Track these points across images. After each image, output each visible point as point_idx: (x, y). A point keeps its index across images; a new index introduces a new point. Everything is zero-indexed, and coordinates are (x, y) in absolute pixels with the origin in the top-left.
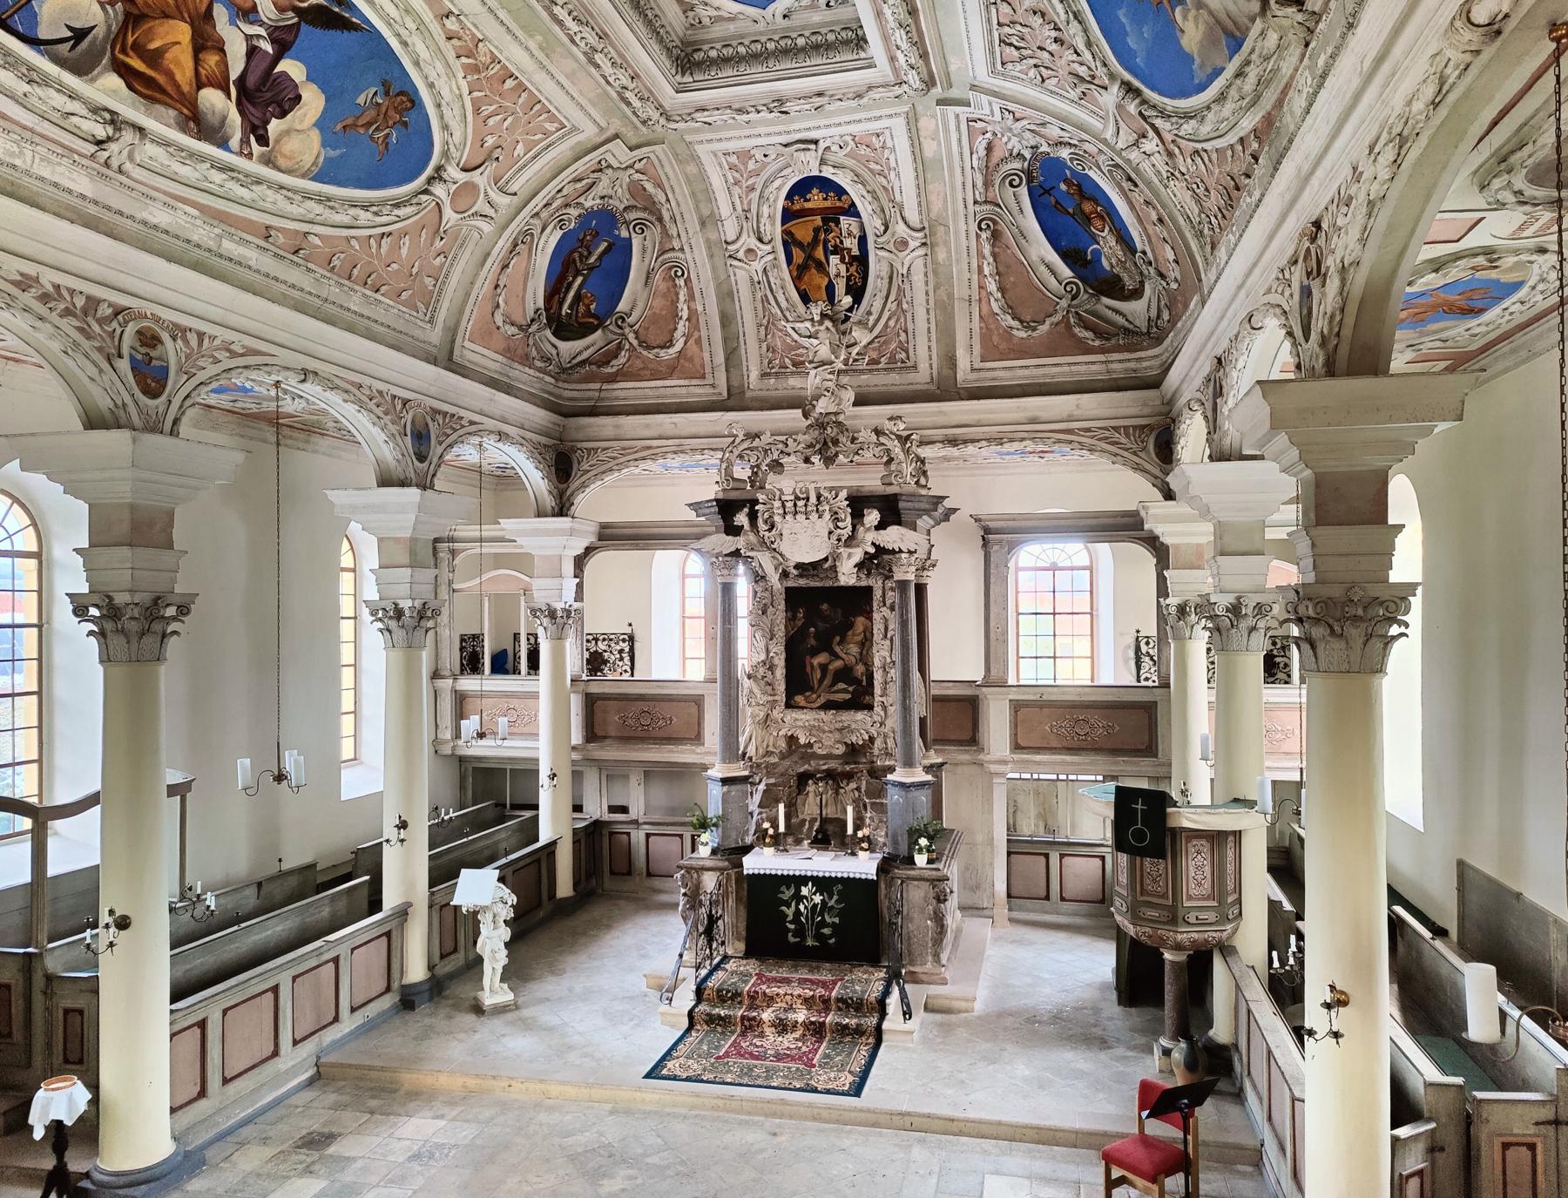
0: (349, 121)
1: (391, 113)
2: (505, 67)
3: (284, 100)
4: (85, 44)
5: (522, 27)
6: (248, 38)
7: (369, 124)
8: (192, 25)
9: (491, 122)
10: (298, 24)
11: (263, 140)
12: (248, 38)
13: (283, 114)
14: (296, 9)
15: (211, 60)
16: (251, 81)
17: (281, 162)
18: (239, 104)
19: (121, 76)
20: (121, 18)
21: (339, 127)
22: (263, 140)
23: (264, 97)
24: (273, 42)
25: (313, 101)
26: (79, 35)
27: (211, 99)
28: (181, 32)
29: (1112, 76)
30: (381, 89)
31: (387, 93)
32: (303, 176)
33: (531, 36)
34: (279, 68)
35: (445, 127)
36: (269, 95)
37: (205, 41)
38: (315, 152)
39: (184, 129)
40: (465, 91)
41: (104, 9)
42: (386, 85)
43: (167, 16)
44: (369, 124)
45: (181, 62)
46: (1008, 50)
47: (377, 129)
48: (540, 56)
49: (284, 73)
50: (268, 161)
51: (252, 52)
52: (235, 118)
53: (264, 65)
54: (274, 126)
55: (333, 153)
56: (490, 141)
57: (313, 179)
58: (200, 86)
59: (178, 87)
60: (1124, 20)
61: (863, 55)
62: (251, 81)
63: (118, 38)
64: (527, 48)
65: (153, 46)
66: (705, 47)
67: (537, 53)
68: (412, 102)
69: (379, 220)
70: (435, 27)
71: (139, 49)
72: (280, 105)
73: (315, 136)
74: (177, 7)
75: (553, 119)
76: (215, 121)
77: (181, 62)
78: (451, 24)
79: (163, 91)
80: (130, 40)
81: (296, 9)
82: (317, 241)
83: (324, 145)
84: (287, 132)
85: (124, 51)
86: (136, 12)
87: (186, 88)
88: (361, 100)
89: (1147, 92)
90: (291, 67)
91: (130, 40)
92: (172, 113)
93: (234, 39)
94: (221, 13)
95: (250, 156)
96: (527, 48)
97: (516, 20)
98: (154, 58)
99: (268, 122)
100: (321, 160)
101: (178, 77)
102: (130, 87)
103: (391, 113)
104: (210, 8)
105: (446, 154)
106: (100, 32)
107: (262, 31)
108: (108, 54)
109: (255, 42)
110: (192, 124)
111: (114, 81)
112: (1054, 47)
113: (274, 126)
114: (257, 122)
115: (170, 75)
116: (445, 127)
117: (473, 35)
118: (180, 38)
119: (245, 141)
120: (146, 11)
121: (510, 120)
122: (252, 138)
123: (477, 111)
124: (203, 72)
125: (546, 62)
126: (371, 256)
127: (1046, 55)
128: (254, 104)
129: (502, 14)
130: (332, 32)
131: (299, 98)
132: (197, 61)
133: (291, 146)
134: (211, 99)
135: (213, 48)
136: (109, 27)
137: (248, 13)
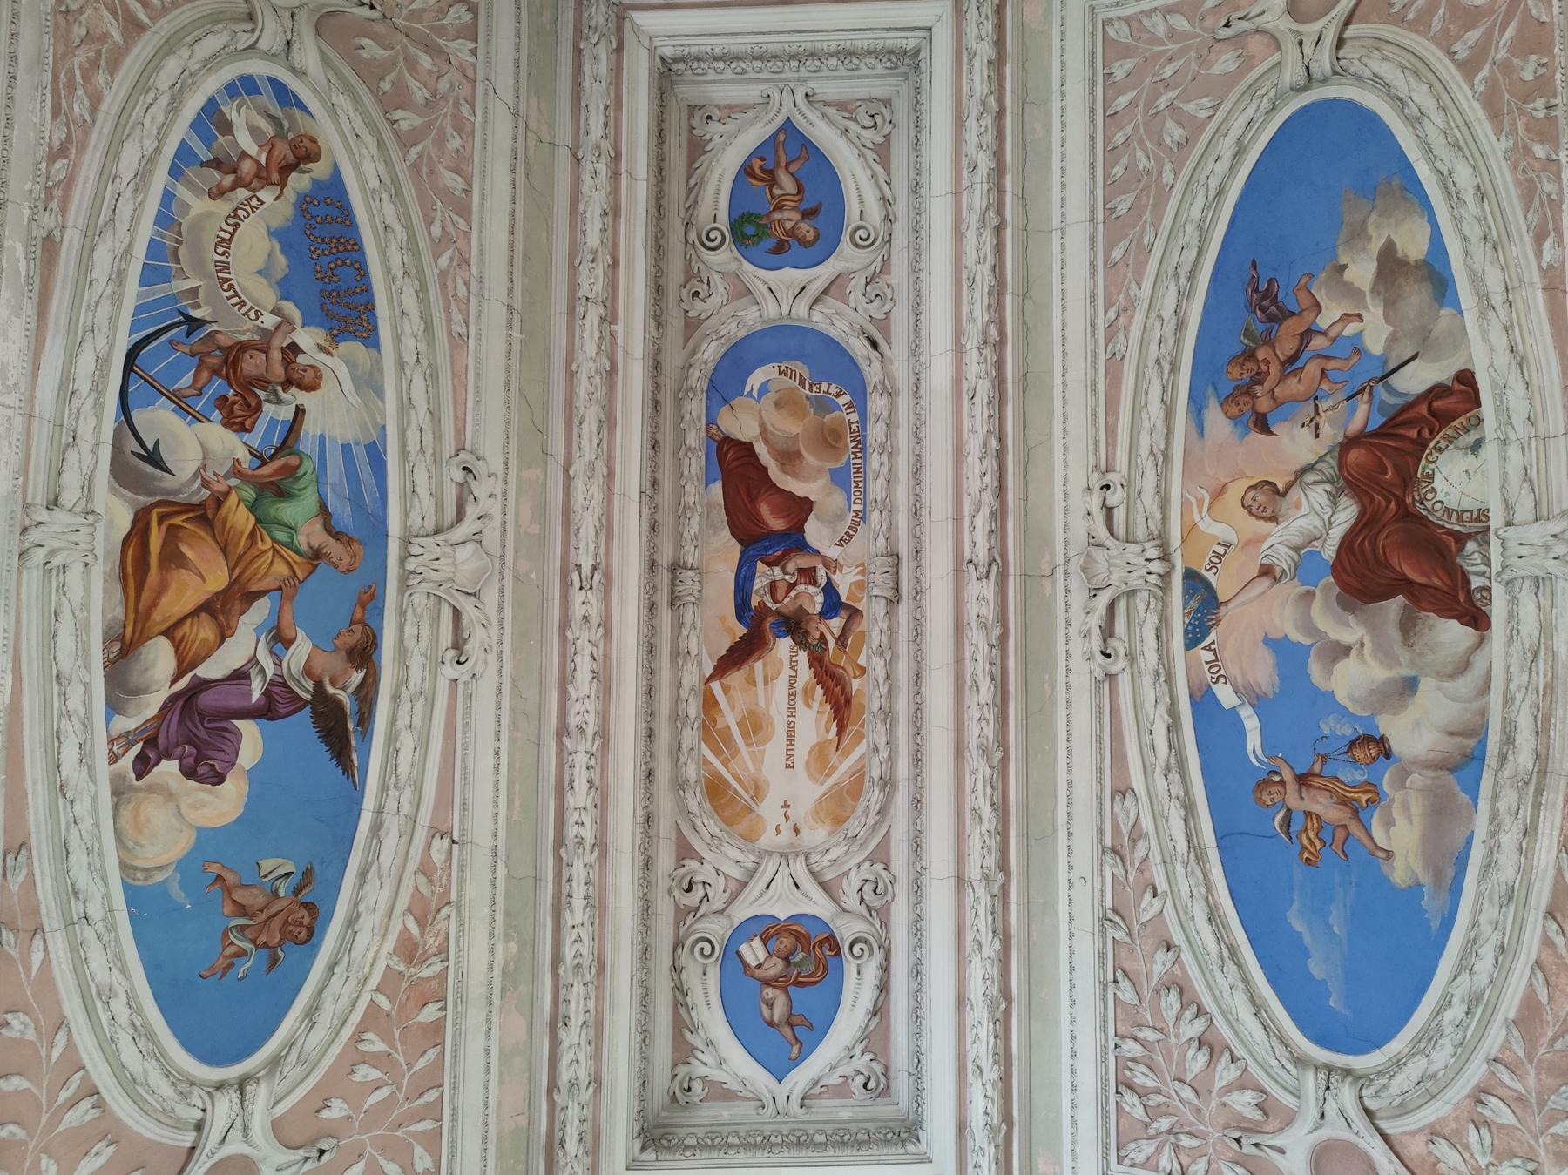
0: (230, 878)
1: (277, 923)
2: (443, 976)
3: (206, 766)
4: (149, 469)
5: (507, 914)
6: (254, 660)
7: (241, 910)
8: (231, 585)
9: (366, 1073)
10: (306, 703)
11: (143, 766)
12: (254, 660)
13: (189, 773)
14: (319, 685)
15: (205, 630)
16: (207, 699)
17: (126, 812)
18: (173, 699)
19: (134, 524)
20: (196, 500)
21: (215, 869)
22: (143, 766)
23: (192, 733)
24: (267, 694)
25: (223, 803)
26: (153, 458)
27: (159, 658)
28: (218, 578)
29: (1300, 1061)
30: (294, 880)
31: (297, 891)
32: (124, 867)
33: (507, 938)
34: (244, 726)
35: (311, 1013)
36: (203, 734)
37: (220, 611)
38: (163, 860)
39: (108, 640)
40: (374, 982)
41: (195, 475)
42: (308, 874)
43: (224, 550)
44: (241, 910)
45: (184, 593)
46: (1130, 1098)
47: (242, 928)
48: (497, 983)
49: (239, 735)
50: (119, 792)
51: (240, 676)
52: (153, 704)
53: (236, 703)
54: (168, 770)
55: (178, 894)
56: (337, 1110)
57: (126, 886)
58: (168, 633)
59: (154, 604)
60: (1298, 925)
61: (910, 1148)
62: (207, 699)
63: (173, 508)
64: (492, 951)
65: (185, 549)
66: (679, 1130)
67: (497, 972)
68: (311, 932)
69: (124, 1039)
70: (421, 835)
71: (172, 534)
72: (197, 761)
73: (181, 844)
74: (240, 558)
75: (432, 1141)
76: (135, 680)
77: (184, 593)
78: (440, 845)
79: (139, 589)
80: (178, 520)
81: (319, 685)
82: (37, 958)
83: (182, 865)
84: (170, 796)
85: (162, 518)
86: (210, 514)
87: (157, 616)
88: (267, 865)
89: (1359, 1062)
90: (251, 738)
91: (178, 520)
92: (119, 612)
93: (243, 646)
94: (260, 611)
95: (114, 758)
96: (492, 951)
97: (508, 895)
98: (173, 558)
99: (168, 757)
100: (159, 877)
101: (164, 600)
102: (126, 541)
103: (277, 923)
104: (260, 594)
105: (275, 1062)
106: (168, 482)
107: (270, 671)
108: (151, 500)
109: (253, 672)
110: (117, 647)
111: (123, 520)
112: (1197, 1062)
113: (168, 770)
114: (161, 740)
115: (162, 588)
116: (311, 1013)
117: (448, 890)
118: (209, 578)
119: (128, 739)
120: (218, 524)
121: (383, 1093)
122: (138, 747)
123: (357, 1037)
124: (186, 627)
125: (496, 1000)
126: (52, 1099)
127: (1187, 1093)
128: (180, 722)
129: (501, 868)
130: (323, 747)
131: (219, 779)
132: (195, 613)
133: (156, 814)
134: (159, 658)
135: (220, 626)
136: (179, 491)
137: (280, 639)
